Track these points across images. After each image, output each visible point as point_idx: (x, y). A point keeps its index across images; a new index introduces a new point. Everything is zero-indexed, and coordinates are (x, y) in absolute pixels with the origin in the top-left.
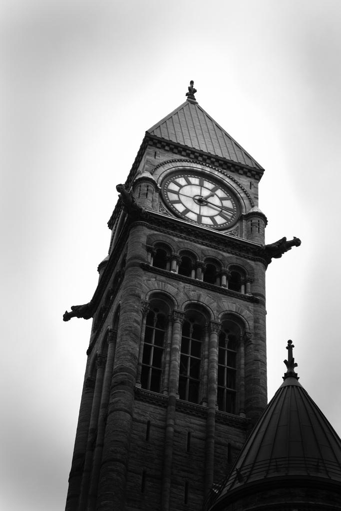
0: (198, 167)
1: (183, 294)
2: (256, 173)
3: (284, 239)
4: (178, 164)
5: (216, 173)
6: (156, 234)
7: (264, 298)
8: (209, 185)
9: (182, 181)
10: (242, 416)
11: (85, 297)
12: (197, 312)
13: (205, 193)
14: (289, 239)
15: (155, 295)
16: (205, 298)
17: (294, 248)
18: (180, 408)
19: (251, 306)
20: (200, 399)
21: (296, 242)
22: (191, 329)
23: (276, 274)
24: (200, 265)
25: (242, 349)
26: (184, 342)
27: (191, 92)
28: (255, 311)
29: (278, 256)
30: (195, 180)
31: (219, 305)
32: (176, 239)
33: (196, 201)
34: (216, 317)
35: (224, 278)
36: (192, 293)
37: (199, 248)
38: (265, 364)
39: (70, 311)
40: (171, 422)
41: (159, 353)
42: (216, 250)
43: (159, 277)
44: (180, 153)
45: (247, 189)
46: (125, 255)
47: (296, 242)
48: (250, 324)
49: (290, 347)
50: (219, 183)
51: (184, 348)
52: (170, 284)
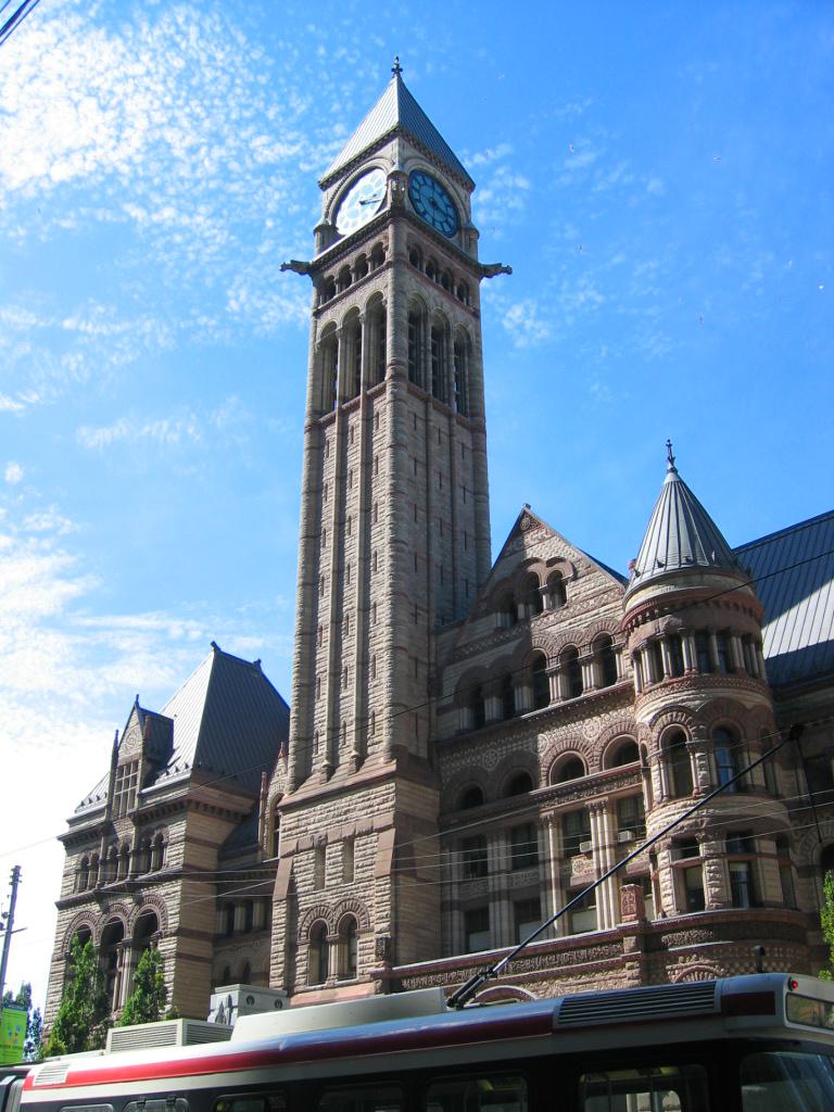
0: (431, 169)
2: (470, 186)
4: (419, 161)
8: (438, 189)
9: (419, 178)
16: (447, 306)
19: (473, 319)
21: (508, 271)
25: (466, 359)
31: (457, 315)
34: (454, 326)
36: (438, 299)
37: (440, 254)
39: (288, 262)
40: (432, 417)
47: (508, 271)
48: (473, 337)
49: (670, 446)
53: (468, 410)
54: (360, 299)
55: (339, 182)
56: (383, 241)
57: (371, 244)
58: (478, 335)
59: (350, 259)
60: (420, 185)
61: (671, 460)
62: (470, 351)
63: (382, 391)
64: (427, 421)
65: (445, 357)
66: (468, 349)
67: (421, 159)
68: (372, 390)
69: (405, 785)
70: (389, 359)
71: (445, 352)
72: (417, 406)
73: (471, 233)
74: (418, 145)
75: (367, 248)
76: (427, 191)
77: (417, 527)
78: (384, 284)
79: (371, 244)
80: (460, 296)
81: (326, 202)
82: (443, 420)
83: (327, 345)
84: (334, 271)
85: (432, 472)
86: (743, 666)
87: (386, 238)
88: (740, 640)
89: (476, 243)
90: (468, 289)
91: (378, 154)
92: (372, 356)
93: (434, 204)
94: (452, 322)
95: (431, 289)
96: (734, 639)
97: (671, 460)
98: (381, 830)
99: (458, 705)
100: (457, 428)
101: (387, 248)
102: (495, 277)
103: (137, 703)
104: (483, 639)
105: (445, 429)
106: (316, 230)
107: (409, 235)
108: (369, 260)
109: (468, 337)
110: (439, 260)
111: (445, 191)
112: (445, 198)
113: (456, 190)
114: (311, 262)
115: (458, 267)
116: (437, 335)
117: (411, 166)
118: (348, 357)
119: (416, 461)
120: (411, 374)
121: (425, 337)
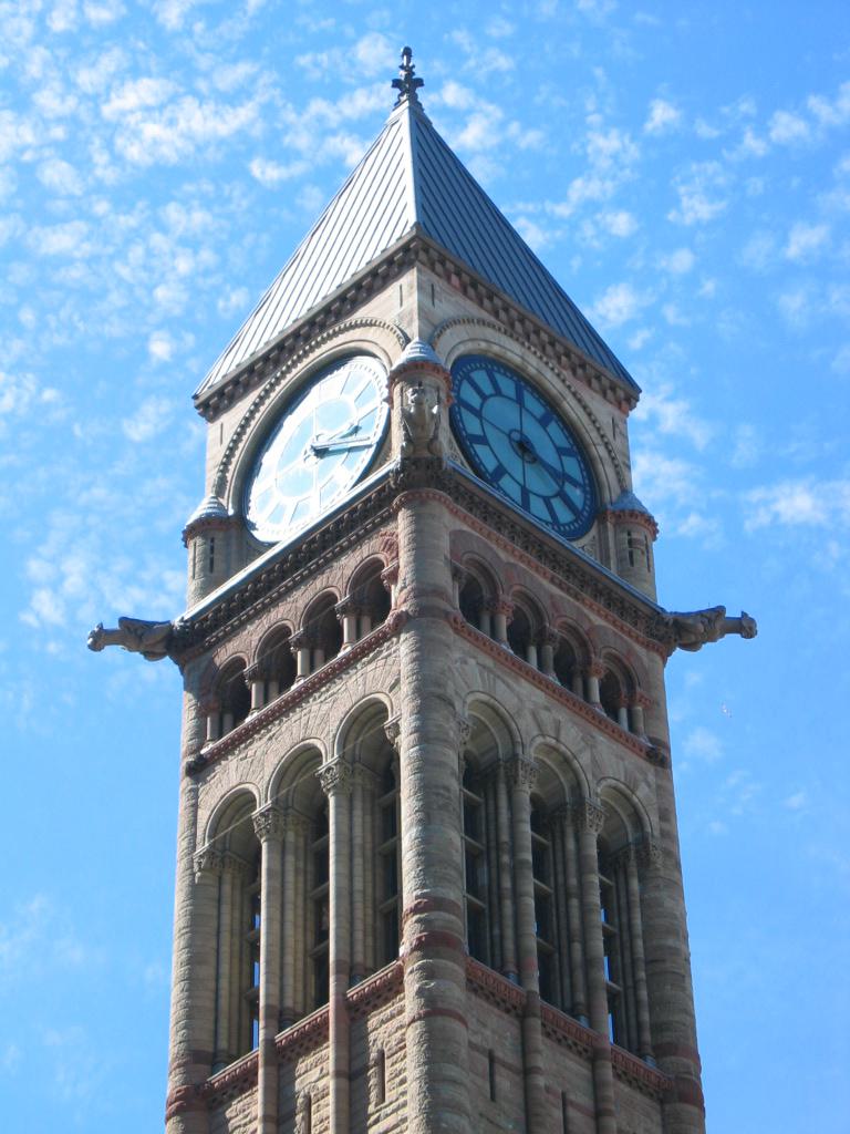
0: (514, 351)
1: (535, 712)
3: (719, 611)
4: (479, 331)
5: (549, 375)
6: (464, 532)
9: (480, 377)
10: (650, 1064)
14: (732, 612)
16: (572, 734)
17: (733, 639)
19: (650, 769)
21: (745, 627)
25: (635, 884)
28: (659, 787)
29: (692, 646)
31: (603, 761)
32: (503, 555)
34: (596, 792)
36: (544, 715)
37: (546, 586)
40: (540, 1062)
42: (577, 603)
47: (745, 627)
48: (652, 821)
52: (504, 682)
53: (647, 1037)
54: (319, 722)
55: (253, 396)
56: (381, 556)
57: (349, 564)
58: (667, 814)
59: (290, 611)
60: (484, 398)
62: (645, 862)
63: (393, 987)
64: (527, 1072)
65: (573, 881)
66: (637, 856)
67: (482, 322)
68: (364, 986)
70: (410, 893)
71: (572, 867)
72: (496, 1031)
73: (635, 524)
74: (471, 286)
75: (338, 577)
76: (503, 412)
78: (388, 676)
79: (349, 564)
81: (216, 453)
82: (575, 1068)
83: (229, 859)
84: (245, 644)
87: (391, 546)
89: (648, 550)
90: (631, 686)
91: (362, 313)
92: (358, 885)
93: (524, 447)
94: (587, 779)
95: (525, 688)
100: (617, 1090)
101: (394, 576)
102: (707, 647)
105: (582, 1098)
106: (191, 532)
107: (456, 536)
108: (345, 610)
109: (638, 821)
110: (545, 603)
111: (553, 411)
112: (553, 428)
113: (586, 406)
114: (176, 623)
115: (598, 621)
116: (547, 818)
117: (455, 343)
118: (290, 893)
120: (474, 937)
121: (514, 823)
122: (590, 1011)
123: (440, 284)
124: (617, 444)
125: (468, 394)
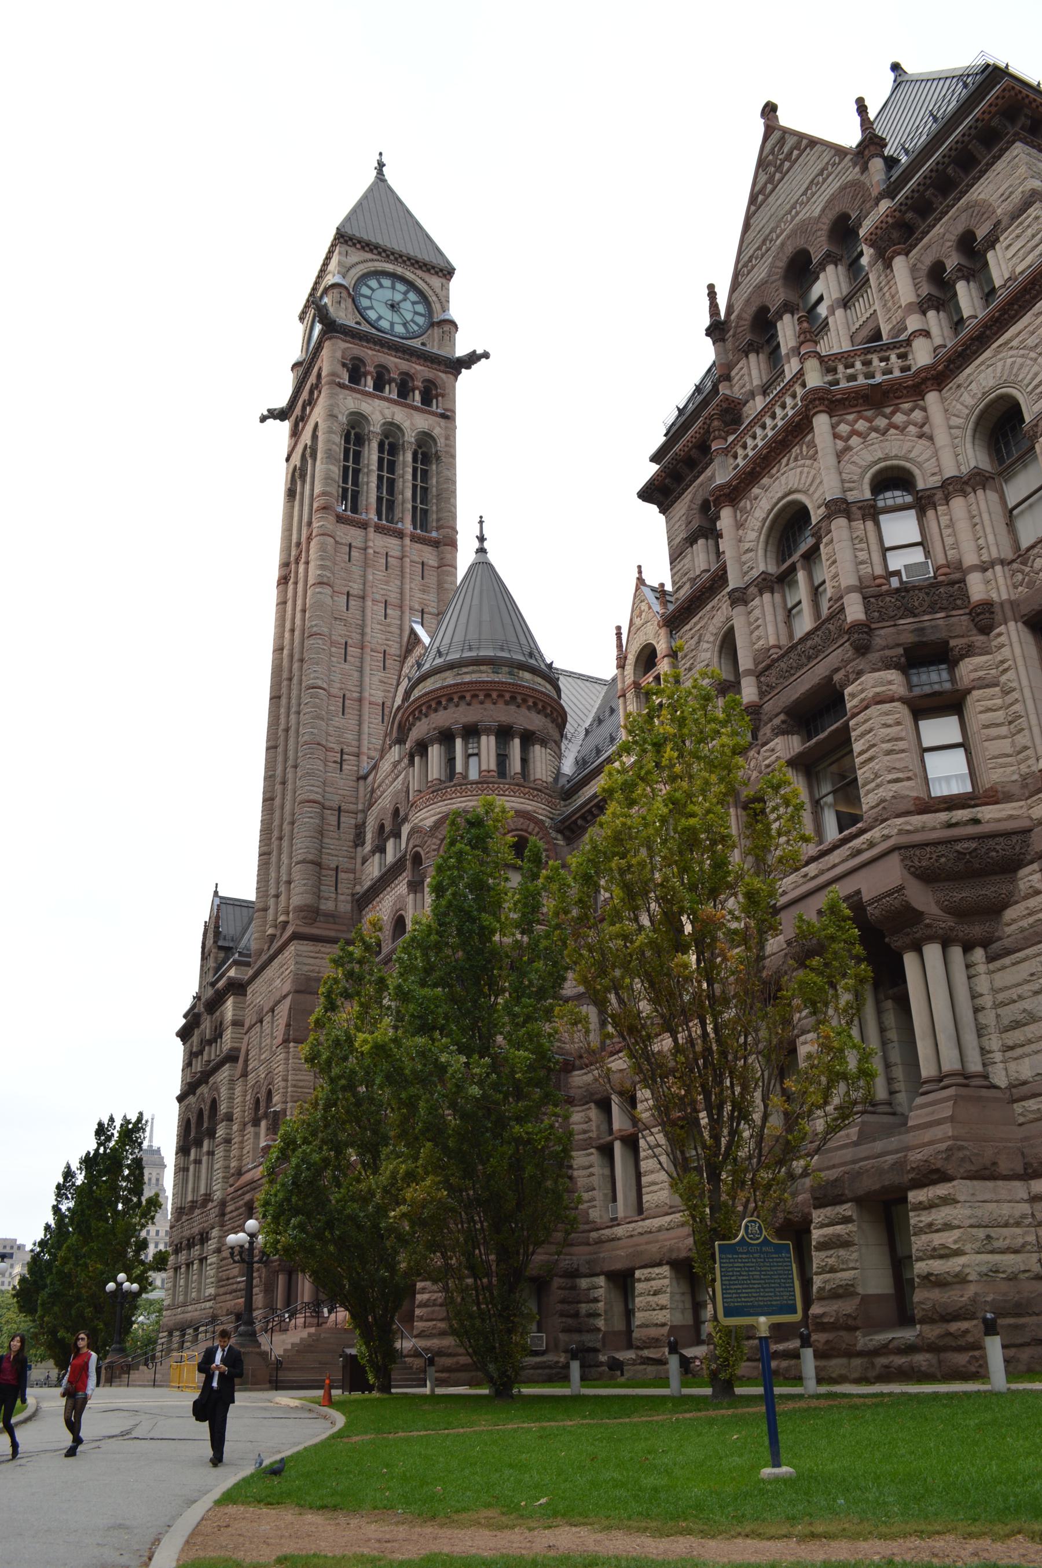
0: (389, 267)
1: (379, 411)
2: (447, 272)
4: (370, 264)
7: (454, 412)
8: (401, 287)
9: (373, 283)
11: (281, 401)
12: (392, 430)
13: (398, 297)
14: (479, 351)
15: (352, 414)
16: (400, 415)
17: (483, 360)
18: (378, 529)
19: (442, 422)
20: (396, 519)
21: (486, 355)
22: (387, 447)
23: (467, 387)
24: (394, 380)
25: (434, 467)
26: (381, 460)
27: (381, 165)
29: (468, 367)
30: (387, 282)
31: (413, 423)
32: (370, 352)
33: (386, 308)
34: (410, 437)
35: (417, 392)
38: (454, 483)
39: (266, 413)
40: (371, 544)
41: (357, 472)
43: (355, 395)
44: (371, 251)
45: (438, 290)
46: (320, 369)
47: (486, 355)
48: (441, 442)
49: (481, 522)
50: (411, 285)
51: (380, 468)
60: (373, 290)
61: (481, 539)
66: (432, 458)
69: (305, 947)
77: (347, 666)
80: (427, 400)
82: (393, 542)
85: (369, 603)
86: (493, 766)
88: (492, 739)
96: (484, 738)
97: (481, 539)
98: (285, 997)
99: (373, 852)
103: (216, 893)
104: (386, 777)
110: (391, 366)
111: (411, 285)
115: (419, 368)
119: (348, 594)
122: (402, 520)
123: (350, 250)
124: (441, 294)
125: (365, 290)
